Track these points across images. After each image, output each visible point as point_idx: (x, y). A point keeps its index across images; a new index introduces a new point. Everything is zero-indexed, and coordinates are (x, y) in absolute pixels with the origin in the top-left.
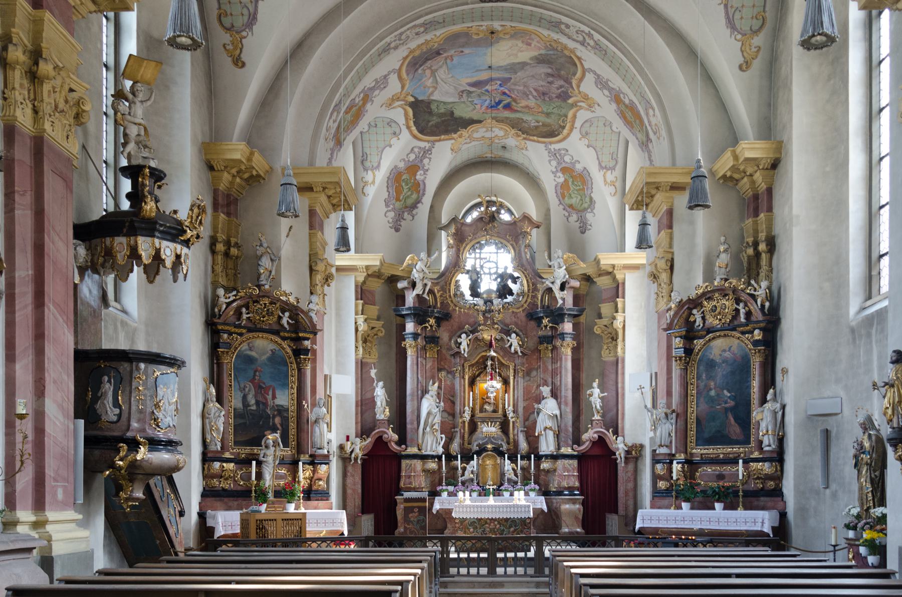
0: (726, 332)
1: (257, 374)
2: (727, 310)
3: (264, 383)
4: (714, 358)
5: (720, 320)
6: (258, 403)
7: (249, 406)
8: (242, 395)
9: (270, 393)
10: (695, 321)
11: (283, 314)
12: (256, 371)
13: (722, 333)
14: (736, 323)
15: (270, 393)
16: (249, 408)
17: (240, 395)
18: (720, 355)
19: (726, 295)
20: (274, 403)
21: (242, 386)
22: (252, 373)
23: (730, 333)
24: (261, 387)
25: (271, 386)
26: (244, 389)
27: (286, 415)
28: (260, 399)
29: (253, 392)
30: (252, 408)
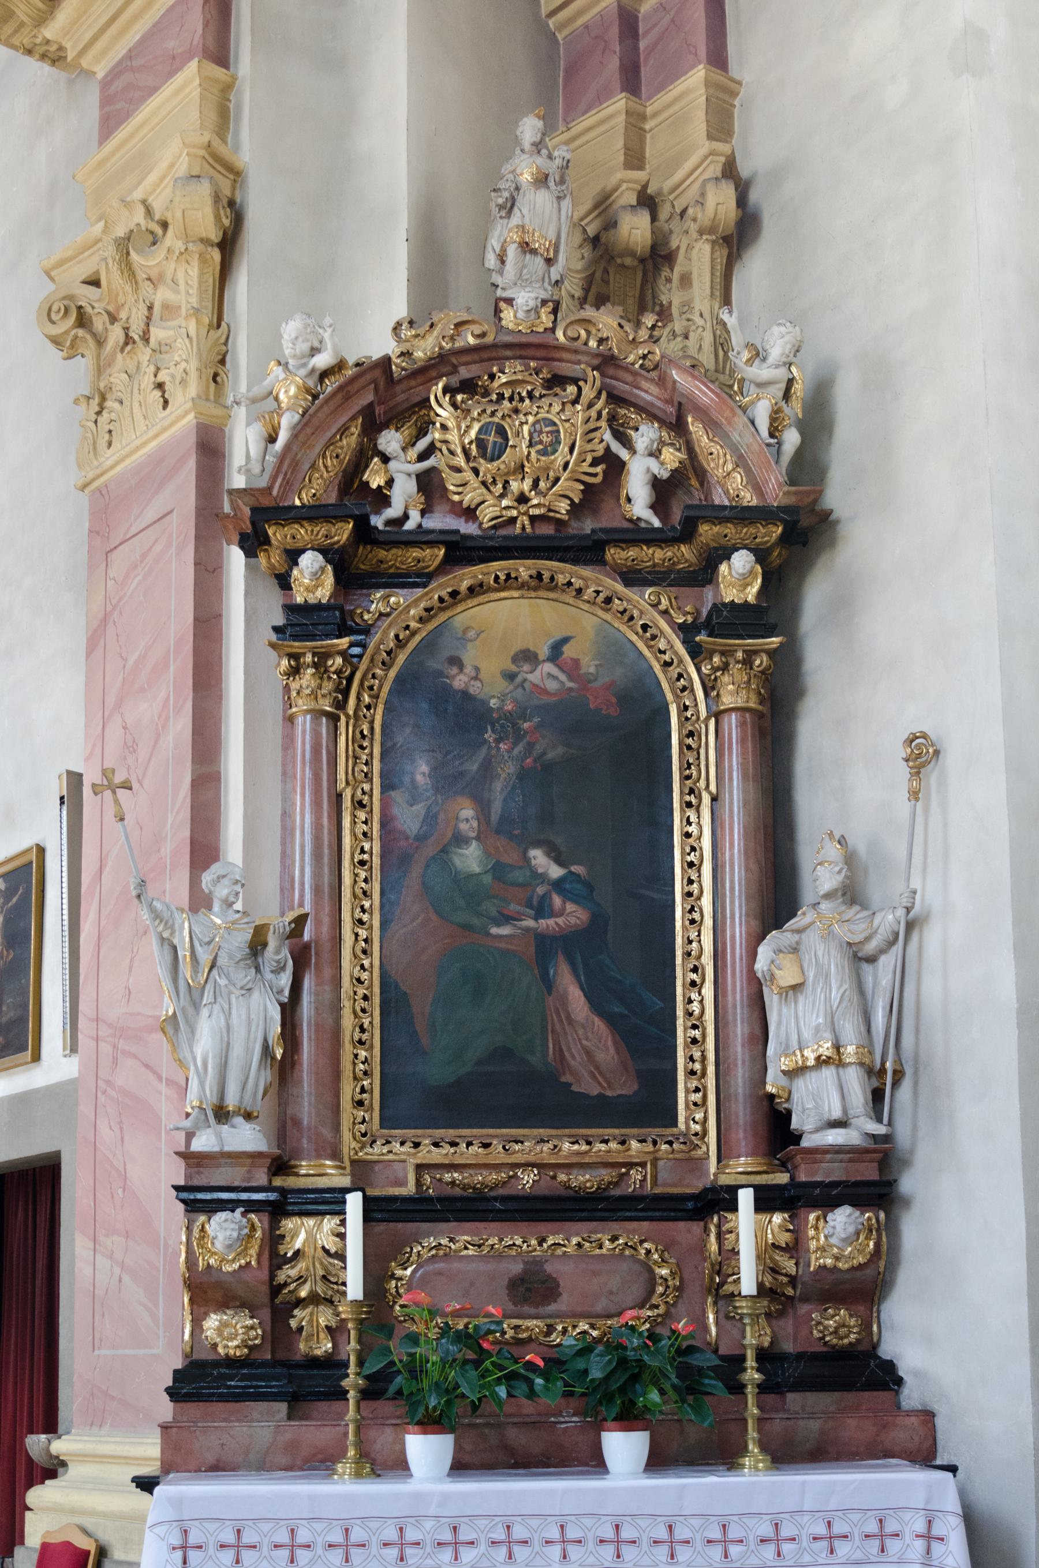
0: (547, 566)
2: (561, 454)
4: (475, 689)
5: (522, 499)
10: (381, 498)
13: (524, 569)
14: (606, 520)
18: (510, 677)
19: (556, 382)
23: (564, 571)
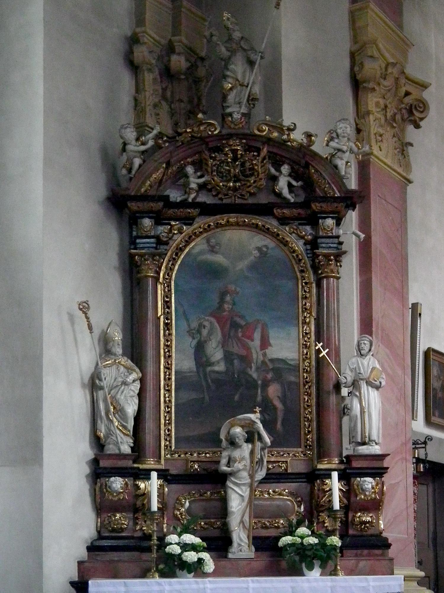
1: (228, 298)
3: (242, 317)
6: (228, 357)
7: (212, 364)
8: (195, 342)
9: (257, 336)
11: (278, 170)
12: (223, 295)
15: (257, 336)
16: (209, 369)
17: (190, 343)
20: (265, 355)
21: (194, 325)
22: (215, 298)
24: (235, 326)
25: (258, 321)
26: (199, 332)
27: (293, 379)
28: (236, 349)
29: (218, 335)
30: (216, 368)
